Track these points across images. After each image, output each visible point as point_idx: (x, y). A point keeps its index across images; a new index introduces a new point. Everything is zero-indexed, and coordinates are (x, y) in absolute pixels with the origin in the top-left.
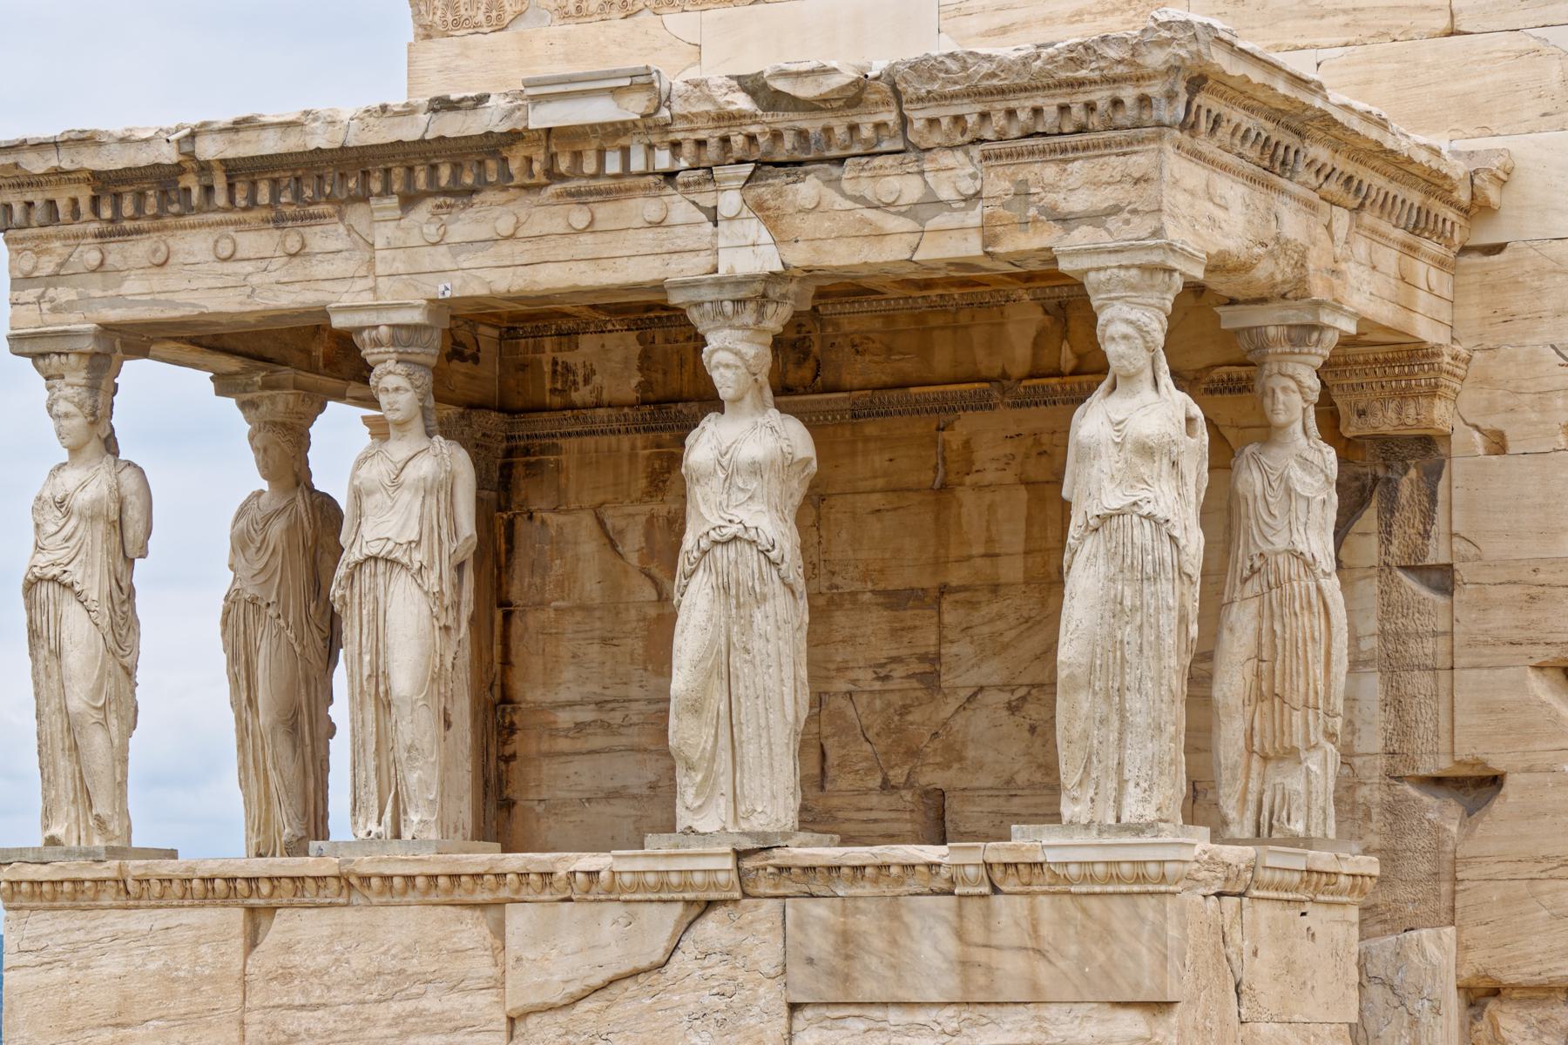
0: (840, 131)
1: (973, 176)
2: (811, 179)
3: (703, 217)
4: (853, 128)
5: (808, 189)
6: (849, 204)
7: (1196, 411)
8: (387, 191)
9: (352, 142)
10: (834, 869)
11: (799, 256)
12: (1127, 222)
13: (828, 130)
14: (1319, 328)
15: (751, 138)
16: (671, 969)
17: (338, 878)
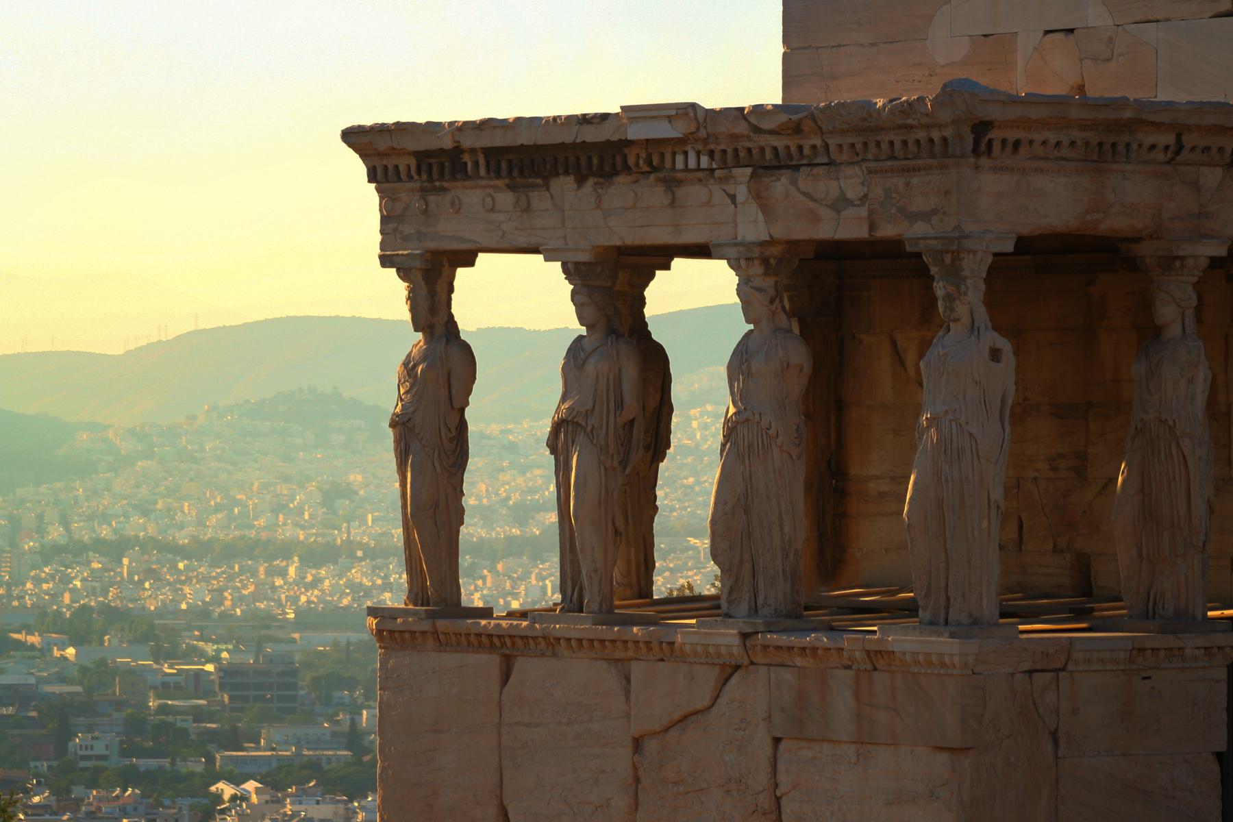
0: (793, 149)
1: (863, 184)
2: (784, 180)
3: (728, 201)
4: (800, 148)
5: (780, 186)
6: (802, 198)
7: (1005, 345)
8: (566, 172)
9: (540, 142)
10: (790, 649)
11: (779, 232)
12: (941, 221)
13: (788, 148)
14: (1182, 258)
15: (749, 150)
16: (715, 710)
17: (544, 637)
